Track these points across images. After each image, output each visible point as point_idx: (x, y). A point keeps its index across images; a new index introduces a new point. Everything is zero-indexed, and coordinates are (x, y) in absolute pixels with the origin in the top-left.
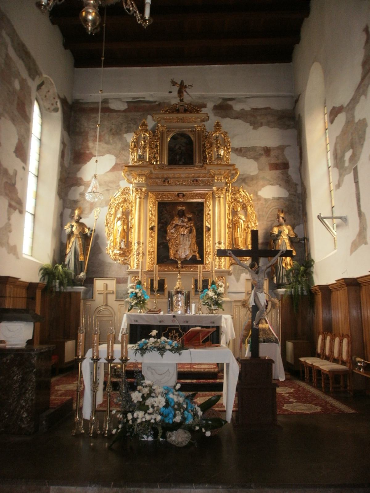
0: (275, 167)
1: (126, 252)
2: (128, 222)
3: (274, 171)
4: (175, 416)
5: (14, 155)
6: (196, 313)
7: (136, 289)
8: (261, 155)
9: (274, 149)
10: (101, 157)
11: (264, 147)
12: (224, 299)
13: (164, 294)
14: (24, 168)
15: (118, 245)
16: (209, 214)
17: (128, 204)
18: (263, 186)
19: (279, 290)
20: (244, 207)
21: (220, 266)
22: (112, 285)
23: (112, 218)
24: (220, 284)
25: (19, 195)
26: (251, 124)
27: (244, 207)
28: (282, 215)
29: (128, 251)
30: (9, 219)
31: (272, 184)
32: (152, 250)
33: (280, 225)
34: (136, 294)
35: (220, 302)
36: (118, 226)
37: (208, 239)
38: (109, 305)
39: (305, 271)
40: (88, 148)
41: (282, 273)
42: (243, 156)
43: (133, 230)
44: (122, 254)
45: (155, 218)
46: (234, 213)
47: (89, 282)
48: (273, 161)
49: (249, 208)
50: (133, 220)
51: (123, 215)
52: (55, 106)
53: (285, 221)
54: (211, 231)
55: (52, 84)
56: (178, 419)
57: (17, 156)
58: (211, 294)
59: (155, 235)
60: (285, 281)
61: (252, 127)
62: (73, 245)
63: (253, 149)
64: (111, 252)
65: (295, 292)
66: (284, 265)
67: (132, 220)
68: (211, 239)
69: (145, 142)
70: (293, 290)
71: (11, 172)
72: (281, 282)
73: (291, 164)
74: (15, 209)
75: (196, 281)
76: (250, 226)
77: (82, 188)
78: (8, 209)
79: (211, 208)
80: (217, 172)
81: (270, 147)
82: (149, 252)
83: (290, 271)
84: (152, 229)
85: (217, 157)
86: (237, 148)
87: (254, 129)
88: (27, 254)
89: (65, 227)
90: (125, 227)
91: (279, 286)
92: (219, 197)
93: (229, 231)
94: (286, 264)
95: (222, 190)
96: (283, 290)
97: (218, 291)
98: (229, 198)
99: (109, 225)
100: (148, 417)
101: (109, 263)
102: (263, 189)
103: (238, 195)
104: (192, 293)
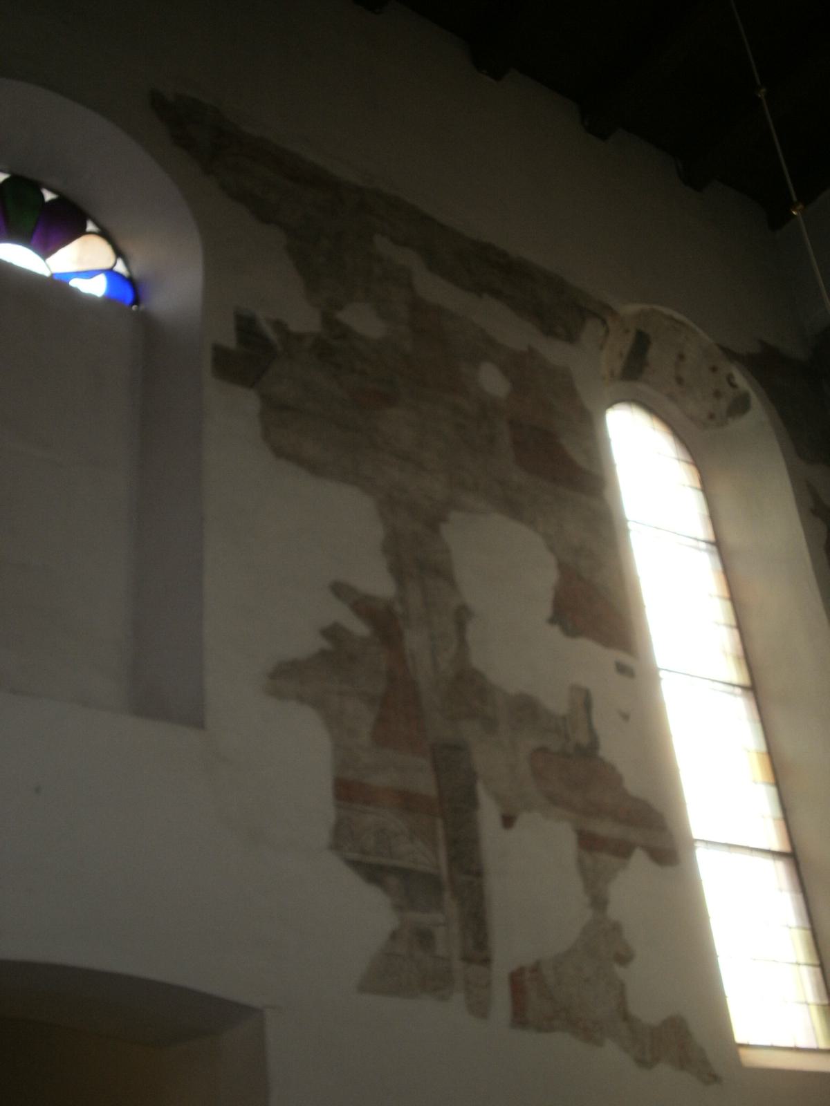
5: (555, 631)
14: (622, 669)
25: (632, 785)
30: (599, 902)
55: (682, 323)
57: (572, 631)
71: (556, 703)
74: (623, 850)
78: (580, 862)
88: (813, 1045)
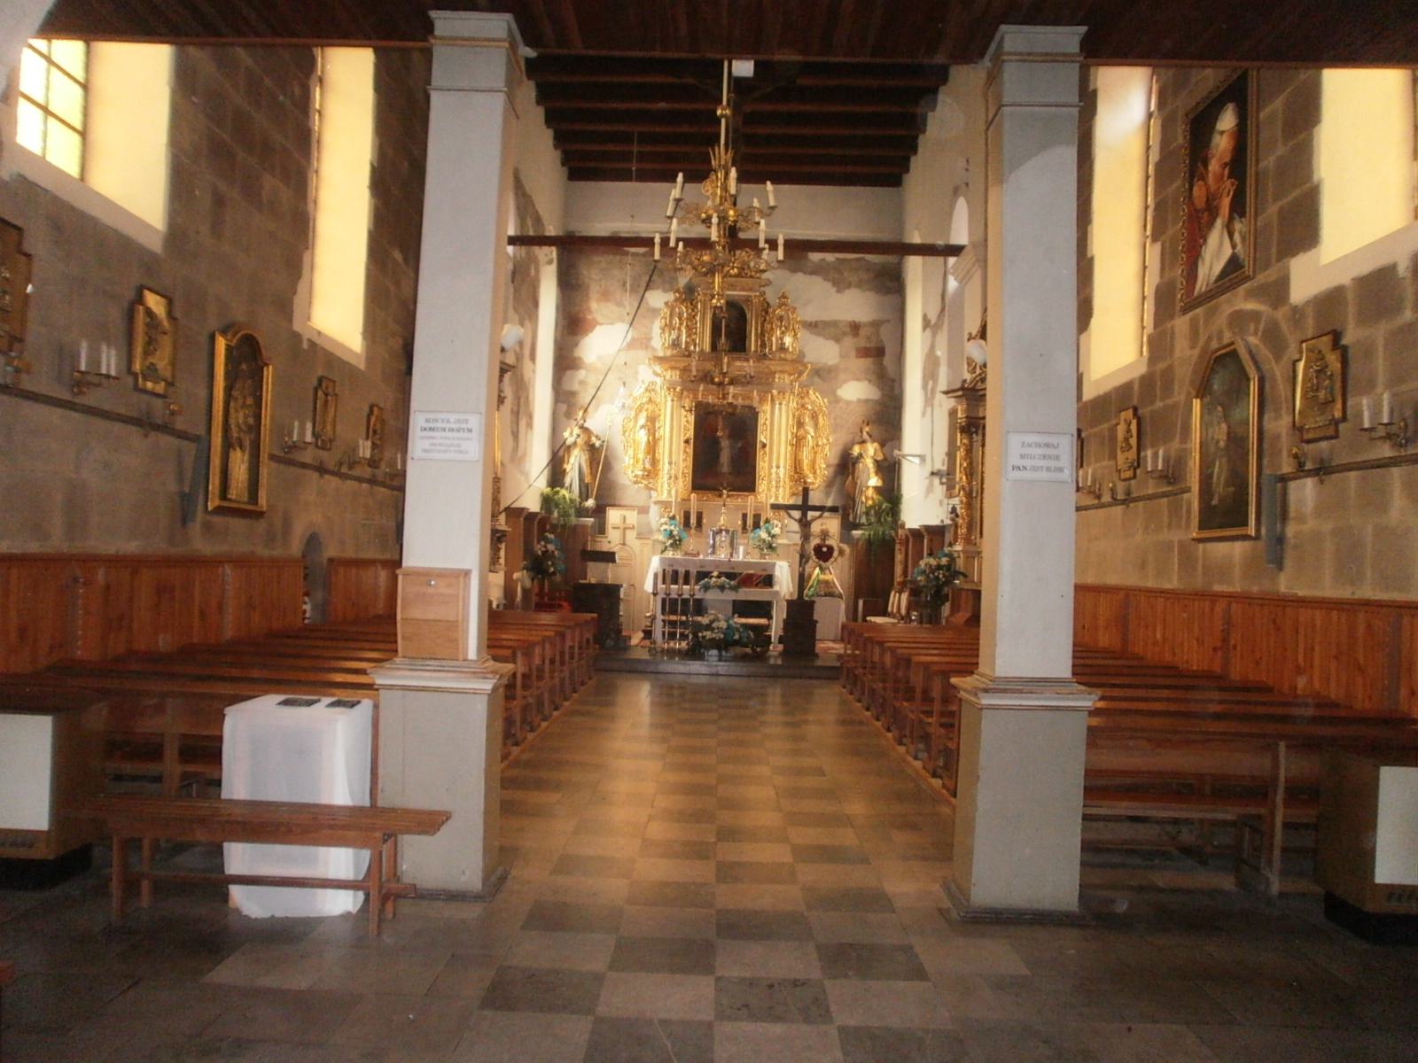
0: (864, 353)
1: (651, 473)
2: (655, 431)
3: (862, 360)
4: (734, 635)
6: (744, 557)
7: (671, 525)
8: (844, 334)
9: (866, 324)
10: (610, 326)
11: (850, 323)
12: (780, 541)
13: (701, 531)
15: (641, 462)
16: (765, 424)
17: (654, 406)
18: (845, 382)
19: (854, 532)
20: (814, 417)
21: (777, 497)
22: (632, 517)
23: (632, 424)
24: (776, 522)
26: (834, 285)
27: (814, 417)
28: (867, 429)
29: (655, 470)
31: (858, 380)
32: (686, 471)
33: (864, 442)
34: (671, 532)
35: (774, 545)
36: (642, 437)
37: (763, 459)
38: (627, 543)
39: (892, 509)
40: (589, 310)
41: (860, 509)
42: (818, 334)
43: (661, 443)
44: (648, 475)
45: (692, 427)
46: (800, 424)
47: (600, 511)
48: (863, 343)
49: (820, 417)
50: (662, 428)
51: (647, 421)
52: (550, 257)
53: (870, 436)
54: (767, 448)
56: (737, 637)
58: (763, 535)
59: (690, 450)
60: (864, 520)
61: (835, 289)
62: (575, 462)
63: (834, 324)
64: (630, 472)
65: (874, 535)
66: (864, 499)
67: (659, 428)
68: (767, 459)
69: (680, 319)
70: (872, 533)
72: (857, 521)
73: (887, 350)
75: (745, 516)
76: (820, 443)
77: (582, 374)
79: (768, 416)
80: (779, 368)
81: (859, 322)
82: (683, 473)
83: (871, 507)
84: (687, 442)
85: (779, 346)
86: (811, 323)
87: (838, 291)
89: (565, 434)
90: (651, 438)
91: (856, 526)
92: (780, 404)
93: (792, 449)
94: (867, 498)
95: (784, 394)
96: (860, 532)
97: (773, 532)
98: (793, 405)
99: (627, 434)
100: (714, 636)
101: (623, 485)
102: (844, 386)
103: (806, 400)
104: (740, 530)
